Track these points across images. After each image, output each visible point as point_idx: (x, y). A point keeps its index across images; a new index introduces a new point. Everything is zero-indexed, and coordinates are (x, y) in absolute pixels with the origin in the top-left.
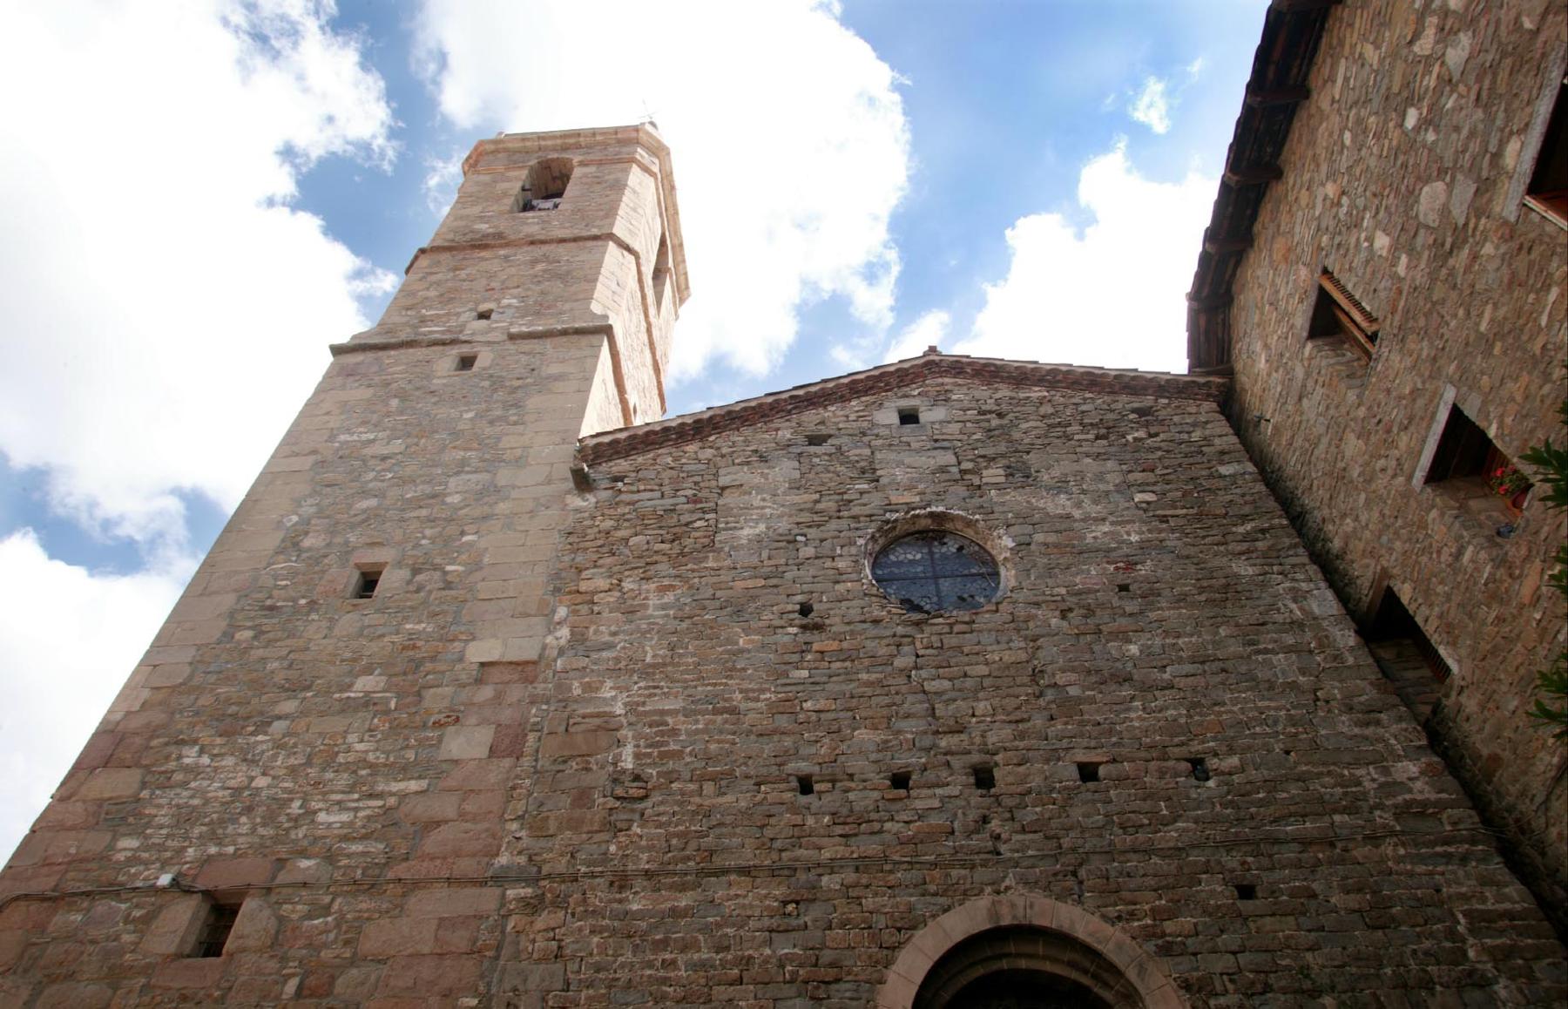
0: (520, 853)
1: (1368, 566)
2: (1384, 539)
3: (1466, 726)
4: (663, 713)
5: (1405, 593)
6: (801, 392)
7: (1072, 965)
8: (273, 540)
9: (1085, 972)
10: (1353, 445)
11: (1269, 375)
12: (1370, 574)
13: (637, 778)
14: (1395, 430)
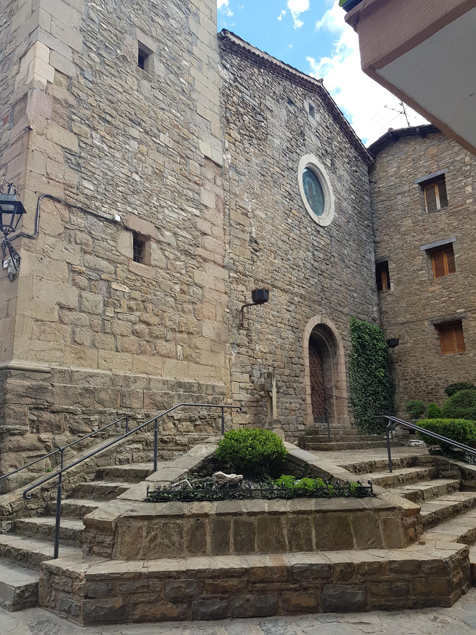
1: (385, 252)
2: (397, 250)
3: (383, 302)
5: (391, 266)
7: (324, 335)
9: (325, 337)
10: (408, 222)
11: (392, 176)
12: (383, 254)
14: (428, 231)
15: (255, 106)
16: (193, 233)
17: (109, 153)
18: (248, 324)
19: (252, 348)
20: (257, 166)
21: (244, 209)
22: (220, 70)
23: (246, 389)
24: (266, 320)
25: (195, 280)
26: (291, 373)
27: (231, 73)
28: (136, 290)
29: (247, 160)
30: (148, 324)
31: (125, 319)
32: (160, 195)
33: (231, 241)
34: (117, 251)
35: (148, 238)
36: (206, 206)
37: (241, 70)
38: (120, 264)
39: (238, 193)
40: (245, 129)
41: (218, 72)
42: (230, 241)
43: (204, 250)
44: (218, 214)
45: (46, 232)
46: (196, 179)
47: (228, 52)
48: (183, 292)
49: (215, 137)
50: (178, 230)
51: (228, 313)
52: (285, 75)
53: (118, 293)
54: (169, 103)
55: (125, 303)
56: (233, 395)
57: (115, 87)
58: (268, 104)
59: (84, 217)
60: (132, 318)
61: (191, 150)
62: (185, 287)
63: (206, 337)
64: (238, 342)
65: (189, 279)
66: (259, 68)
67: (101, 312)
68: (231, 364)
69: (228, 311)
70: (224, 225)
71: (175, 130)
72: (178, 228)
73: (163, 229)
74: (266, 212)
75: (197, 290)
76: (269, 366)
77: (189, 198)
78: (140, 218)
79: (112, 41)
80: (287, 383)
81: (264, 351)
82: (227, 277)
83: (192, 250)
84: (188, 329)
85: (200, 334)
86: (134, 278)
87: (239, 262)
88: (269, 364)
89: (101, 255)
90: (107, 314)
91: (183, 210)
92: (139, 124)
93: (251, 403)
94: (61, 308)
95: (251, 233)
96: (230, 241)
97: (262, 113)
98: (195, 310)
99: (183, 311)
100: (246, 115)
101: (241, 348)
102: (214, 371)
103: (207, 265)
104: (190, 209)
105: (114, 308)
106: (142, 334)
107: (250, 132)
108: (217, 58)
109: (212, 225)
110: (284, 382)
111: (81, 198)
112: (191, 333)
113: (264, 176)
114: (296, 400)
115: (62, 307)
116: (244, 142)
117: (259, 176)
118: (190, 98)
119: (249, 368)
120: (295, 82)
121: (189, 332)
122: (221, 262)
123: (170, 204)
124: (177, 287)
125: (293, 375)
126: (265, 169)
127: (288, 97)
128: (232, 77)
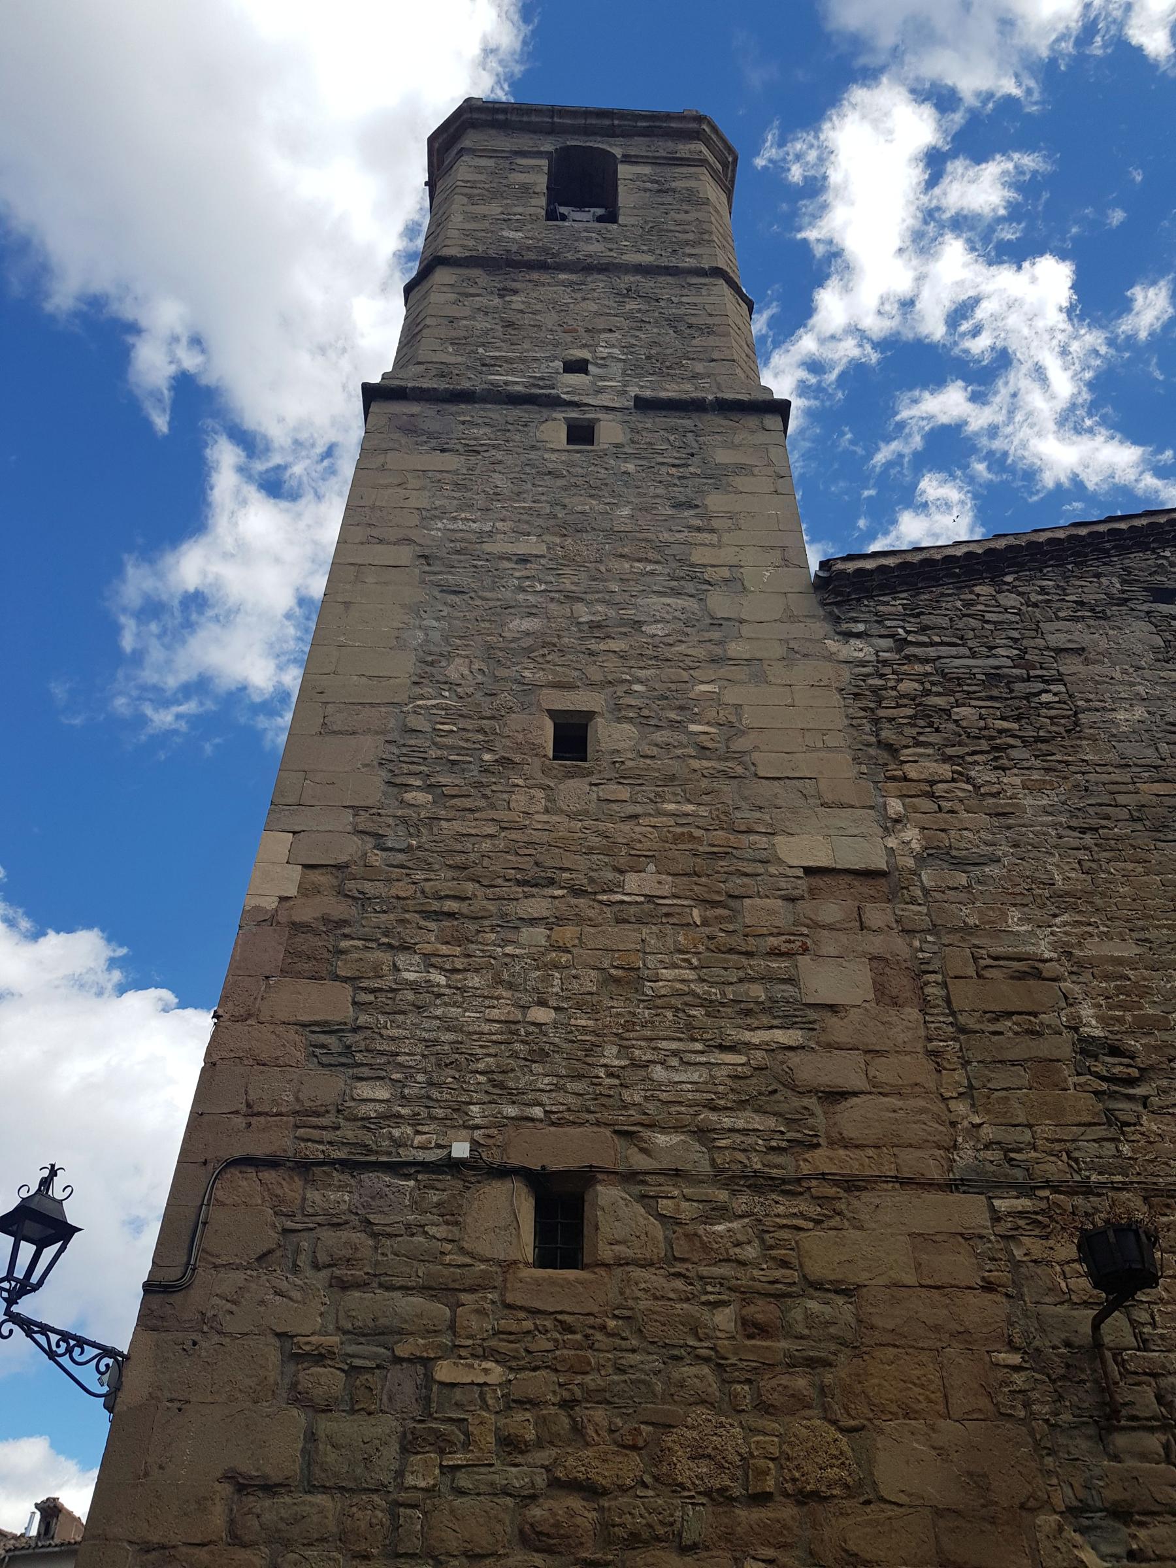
0: (987, 1147)
4: (1119, 961)
6: (1123, 526)
8: (404, 666)
13: (1115, 1051)
15: (997, 668)
16: (784, 1107)
17: (448, 986)
18: (1159, 1398)
20: (1050, 814)
21: (1020, 960)
22: (834, 650)
25: (807, 1270)
27: (881, 636)
28: (535, 1369)
29: (998, 815)
30: (590, 1490)
31: (484, 1488)
32: (632, 1035)
33: (975, 1083)
34: (463, 1251)
35: (587, 1177)
36: (831, 1006)
37: (922, 613)
38: (471, 1290)
39: (970, 921)
40: (967, 741)
41: (830, 657)
42: (971, 1087)
43: (842, 1152)
44: (892, 1015)
45: (218, 1261)
46: (773, 941)
47: (858, 600)
48: (753, 1328)
49: (842, 806)
50: (713, 1117)
51: (1017, 1368)
52: (1108, 546)
53: (458, 1394)
54: (652, 795)
55: (485, 1428)
57: (473, 832)
58: (1054, 640)
59: (353, 1182)
60: (516, 1477)
61: (747, 875)
62: (761, 1310)
63: (903, 1499)
64: (1113, 1494)
65: (778, 1273)
66: (996, 580)
67: (385, 1477)
69: (1016, 1359)
70: (930, 1040)
71: (680, 847)
72: (714, 1109)
73: (646, 1133)
74: (1135, 935)
75: (827, 1309)
77: (752, 1005)
78: (553, 1124)
79: (469, 745)
82: (984, 1219)
83: (786, 1166)
84: (794, 1480)
85: (864, 1491)
86: (528, 1325)
87: (1035, 1148)
89: (398, 1281)
90: (410, 1480)
91: (731, 1049)
92: (552, 882)
94: (241, 1489)
95: (1076, 1029)
96: (971, 1087)
97: (1032, 673)
98: (823, 1390)
99: (764, 1408)
100: (964, 705)
101: (1141, 1524)
103: (862, 1204)
104: (756, 1037)
105: (442, 1452)
106: (562, 1537)
107: (993, 738)
108: (820, 628)
109: (868, 1057)
111: (349, 1132)
112: (816, 1496)
113: (1096, 830)
115: (241, 1485)
116: (973, 774)
117: (1072, 838)
118: (729, 756)
120: (1168, 541)
121: (801, 1492)
122: (935, 1174)
123: (674, 1045)
124: (724, 1319)
126: (1091, 810)
127: (1146, 590)
128: (887, 643)
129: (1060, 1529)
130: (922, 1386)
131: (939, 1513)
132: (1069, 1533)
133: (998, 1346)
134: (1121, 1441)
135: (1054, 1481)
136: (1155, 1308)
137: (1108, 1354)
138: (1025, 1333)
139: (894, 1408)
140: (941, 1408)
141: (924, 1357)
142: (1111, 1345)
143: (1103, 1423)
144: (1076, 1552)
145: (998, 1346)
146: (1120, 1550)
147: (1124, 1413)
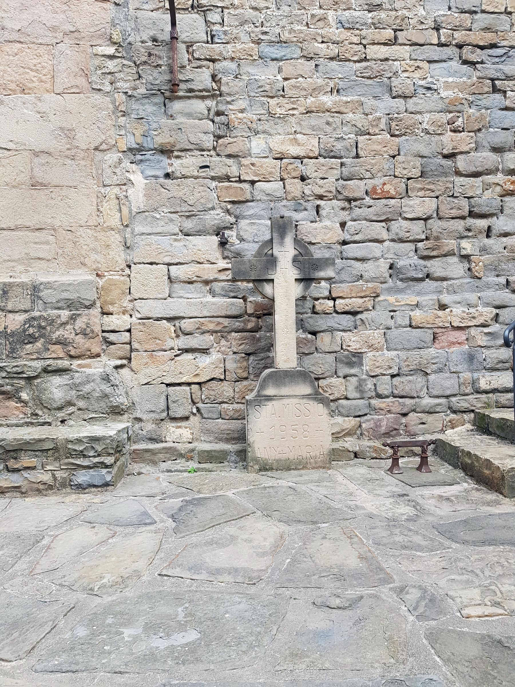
18: (214, 77)
19: (230, 150)
23: (207, 282)
24: (305, 45)
26: (442, 208)
51: (111, 57)
56: (137, 303)
63: (11, 146)
64: (160, 140)
68: (125, 210)
69: (111, 50)
76: (321, 197)
80: (420, 245)
81: (295, 150)
88: (320, 191)
93: (226, 322)
101: (178, 157)
102: (47, 243)
110: (401, 241)
114: (472, 297)
119: (217, 217)
125: (455, 213)
129: (120, 161)
130: (37, 71)
131: (36, 154)
132: (126, 164)
133: (99, 42)
134: (177, 106)
135: (123, 132)
136: (226, 11)
137: (182, 47)
138: (123, 32)
139: (13, 86)
140: (48, 86)
141: (42, 50)
142: (186, 39)
143: (168, 94)
144: (127, 174)
145: (99, 42)
146: (160, 173)
147: (182, 86)
